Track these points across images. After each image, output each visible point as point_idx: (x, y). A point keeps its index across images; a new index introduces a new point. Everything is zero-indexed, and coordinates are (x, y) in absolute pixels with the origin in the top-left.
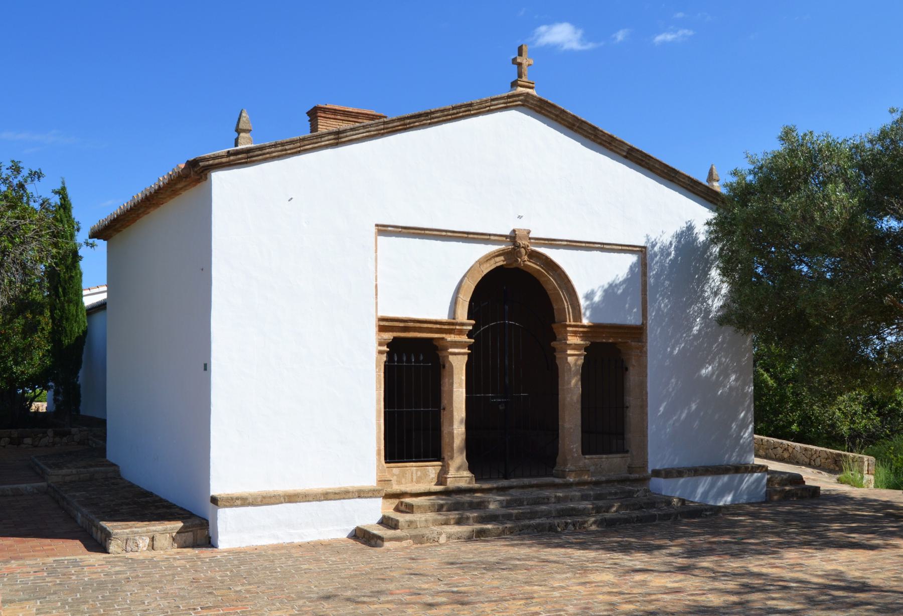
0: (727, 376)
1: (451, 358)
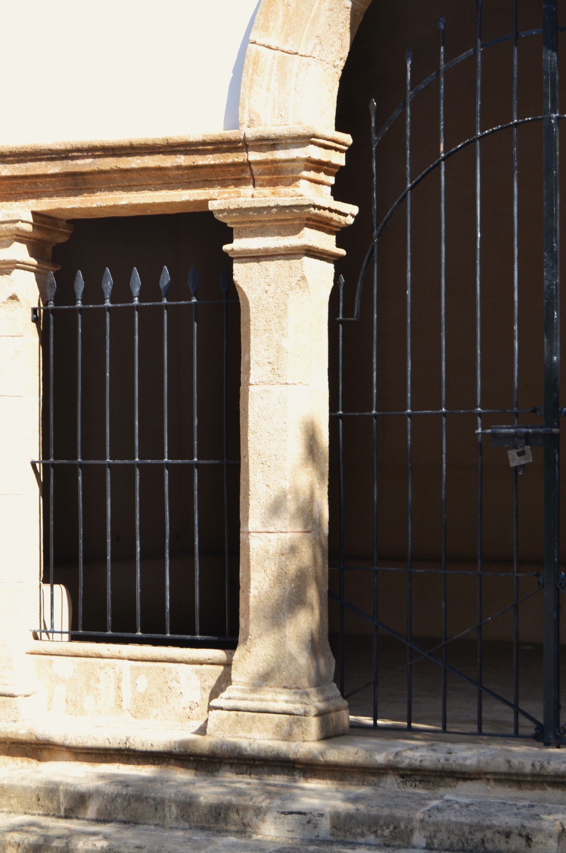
1: (241, 273)
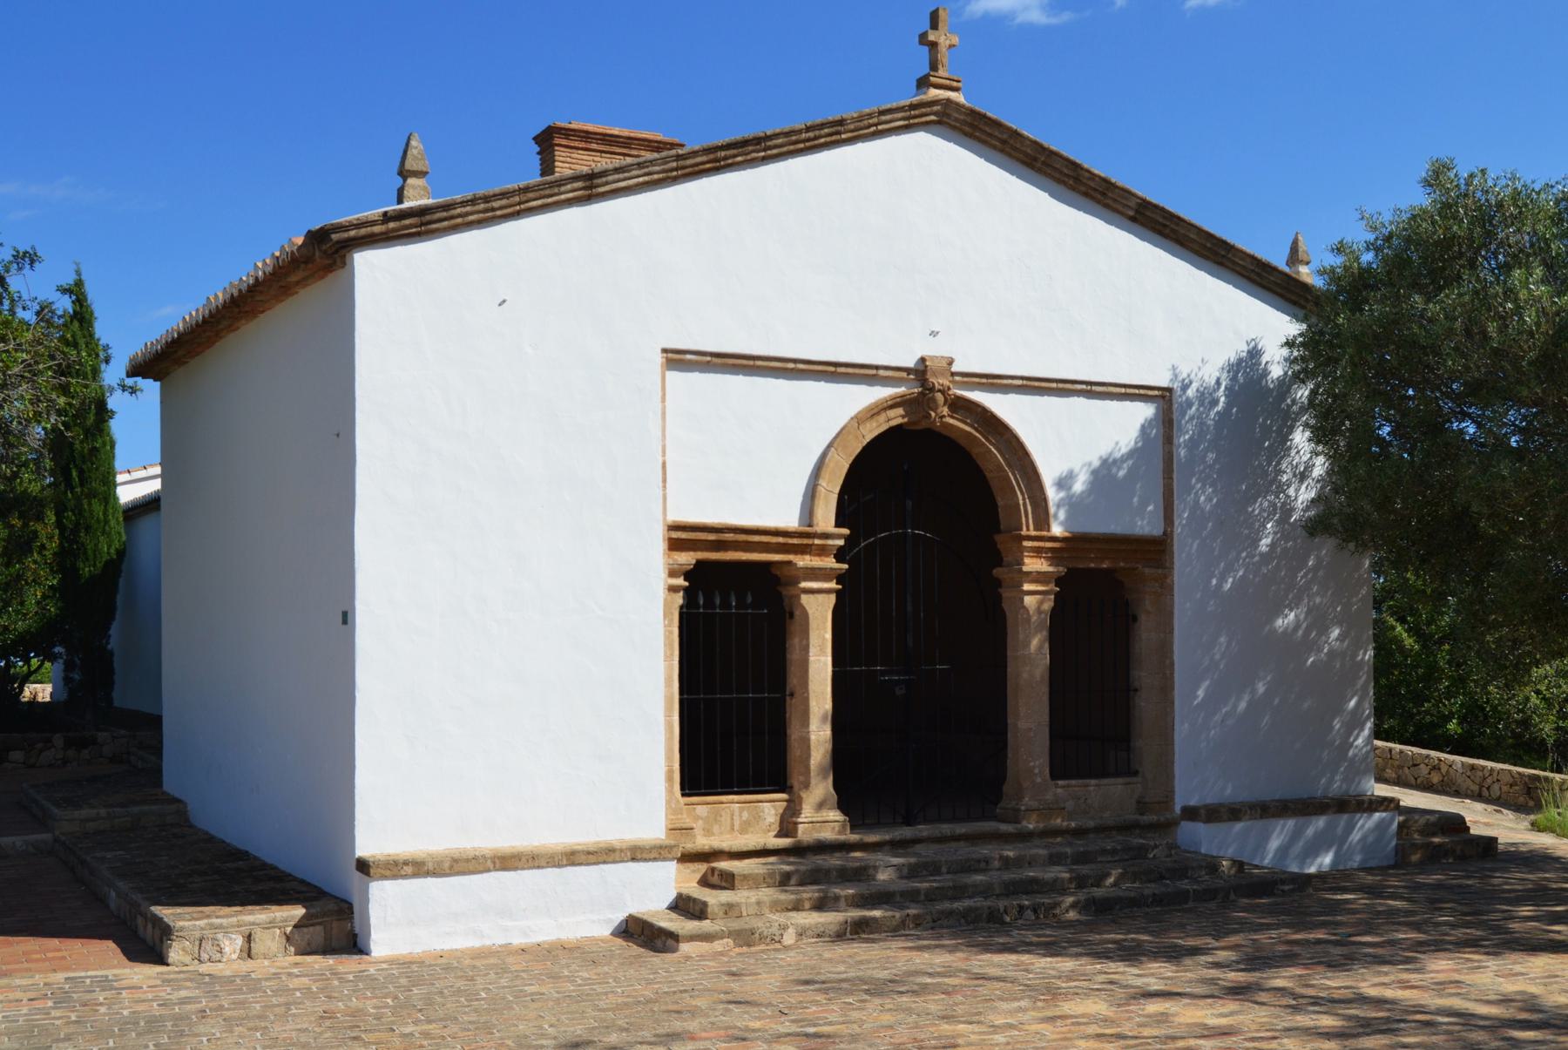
0: (1324, 631)
1: (805, 599)
